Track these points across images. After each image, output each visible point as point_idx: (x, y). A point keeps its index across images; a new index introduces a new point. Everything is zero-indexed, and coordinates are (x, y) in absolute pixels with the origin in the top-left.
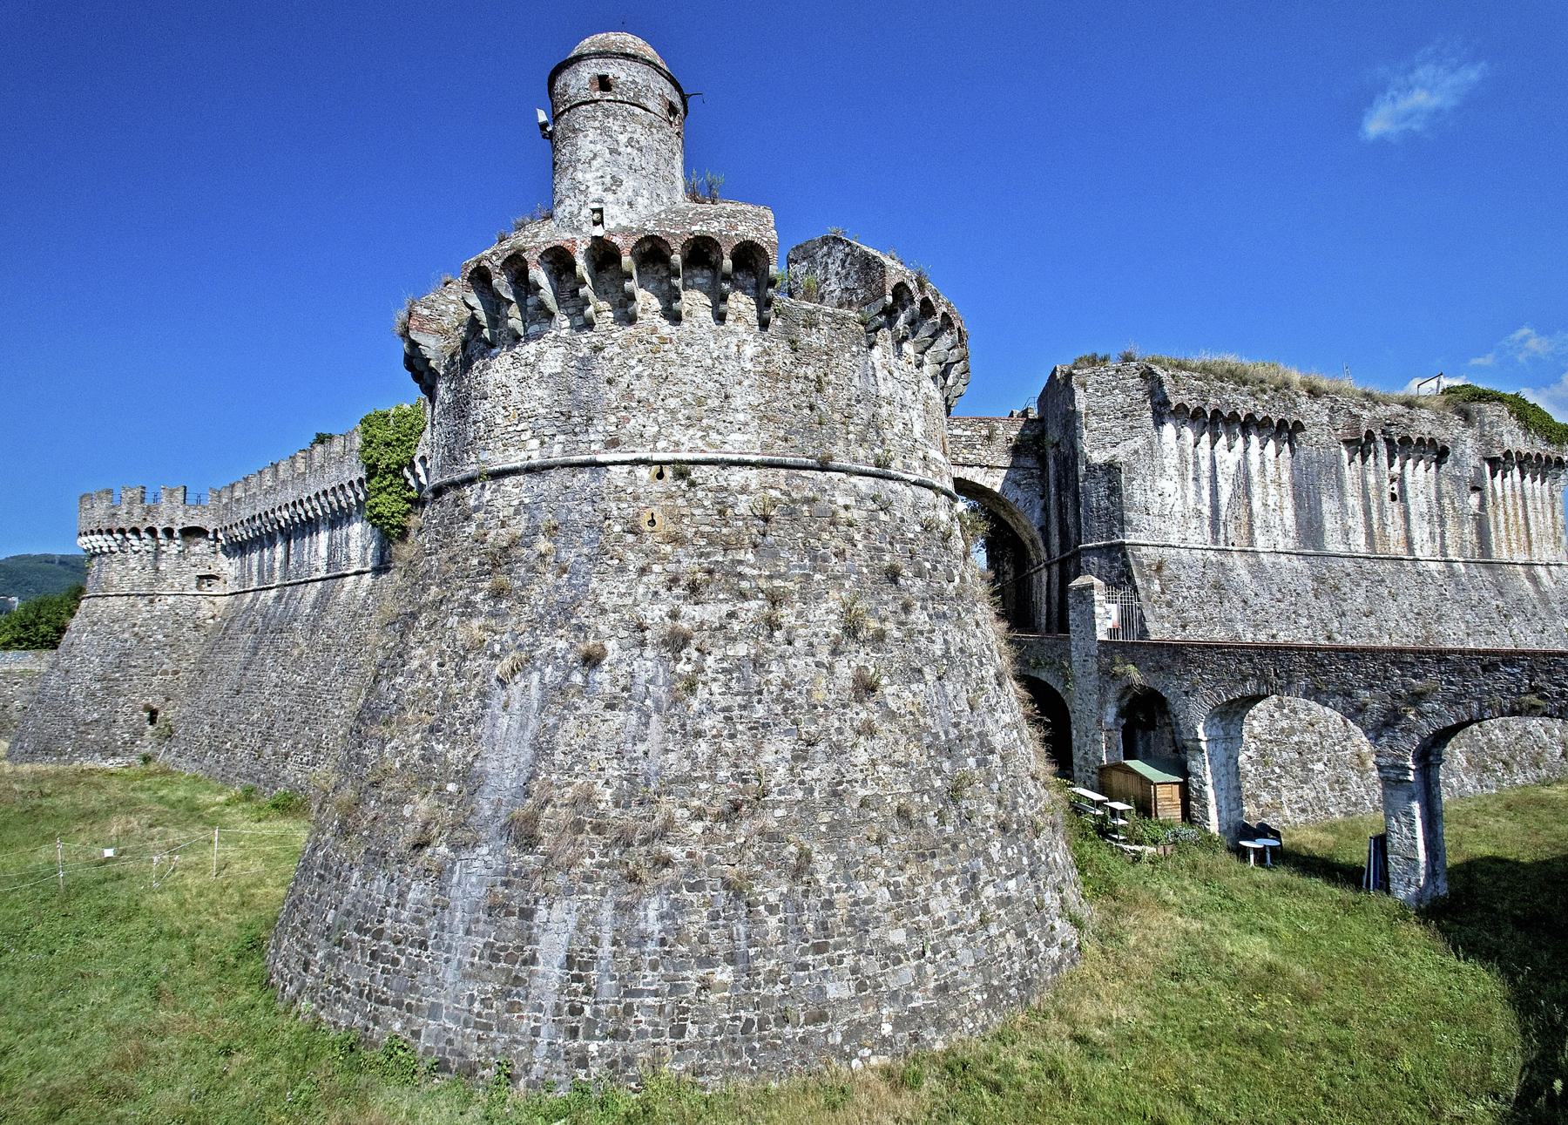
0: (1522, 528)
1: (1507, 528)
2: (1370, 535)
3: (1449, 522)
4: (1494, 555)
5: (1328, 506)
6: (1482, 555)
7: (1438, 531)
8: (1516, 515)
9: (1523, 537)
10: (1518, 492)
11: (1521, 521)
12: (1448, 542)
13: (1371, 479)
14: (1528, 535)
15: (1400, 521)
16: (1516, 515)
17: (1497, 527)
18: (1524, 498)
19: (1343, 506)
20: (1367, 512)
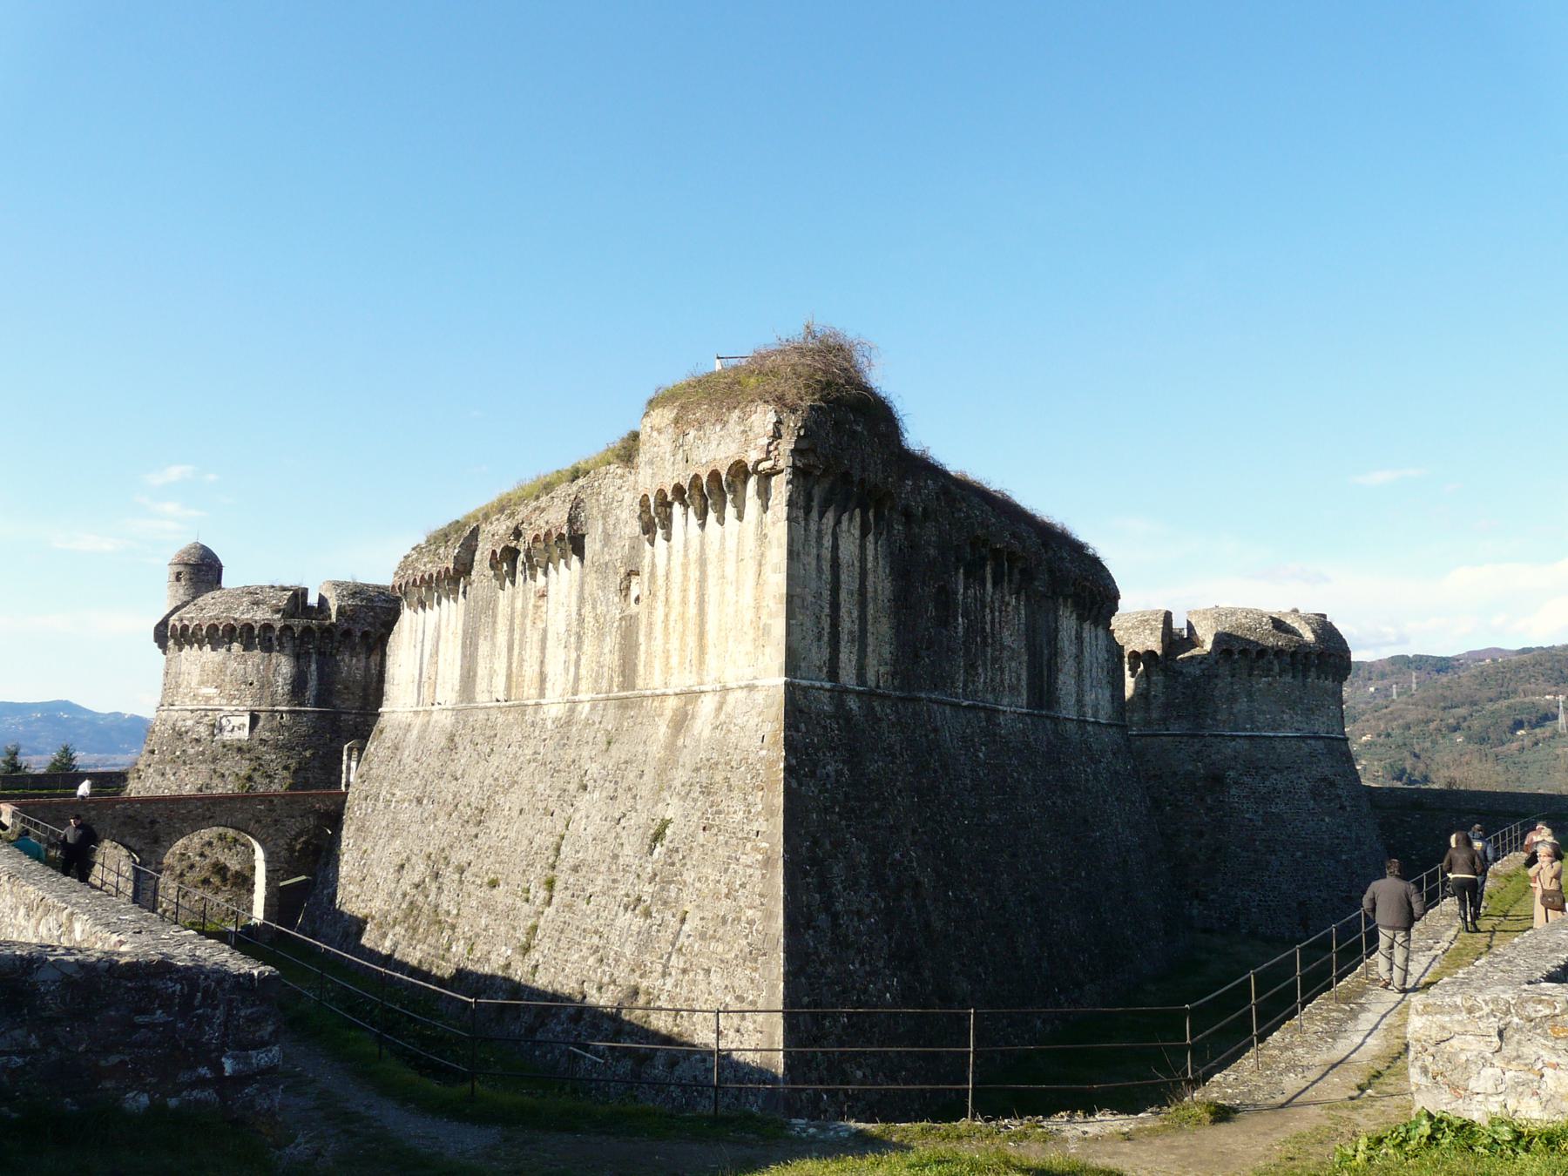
0: (692, 629)
1: (666, 627)
2: (509, 677)
3: (586, 641)
4: (640, 683)
5: (484, 648)
6: (623, 687)
7: (573, 656)
8: (684, 602)
9: (692, 641)
10: (693, 555)
11: (692, 610)
12: (583, 672)
13: (519, 604)
14: (702, 635)
15: (537, 653)
16: (684, 602)
17: (649, 635)
18: (702, 562)
19: (494, 645)
20: (510, 649)
